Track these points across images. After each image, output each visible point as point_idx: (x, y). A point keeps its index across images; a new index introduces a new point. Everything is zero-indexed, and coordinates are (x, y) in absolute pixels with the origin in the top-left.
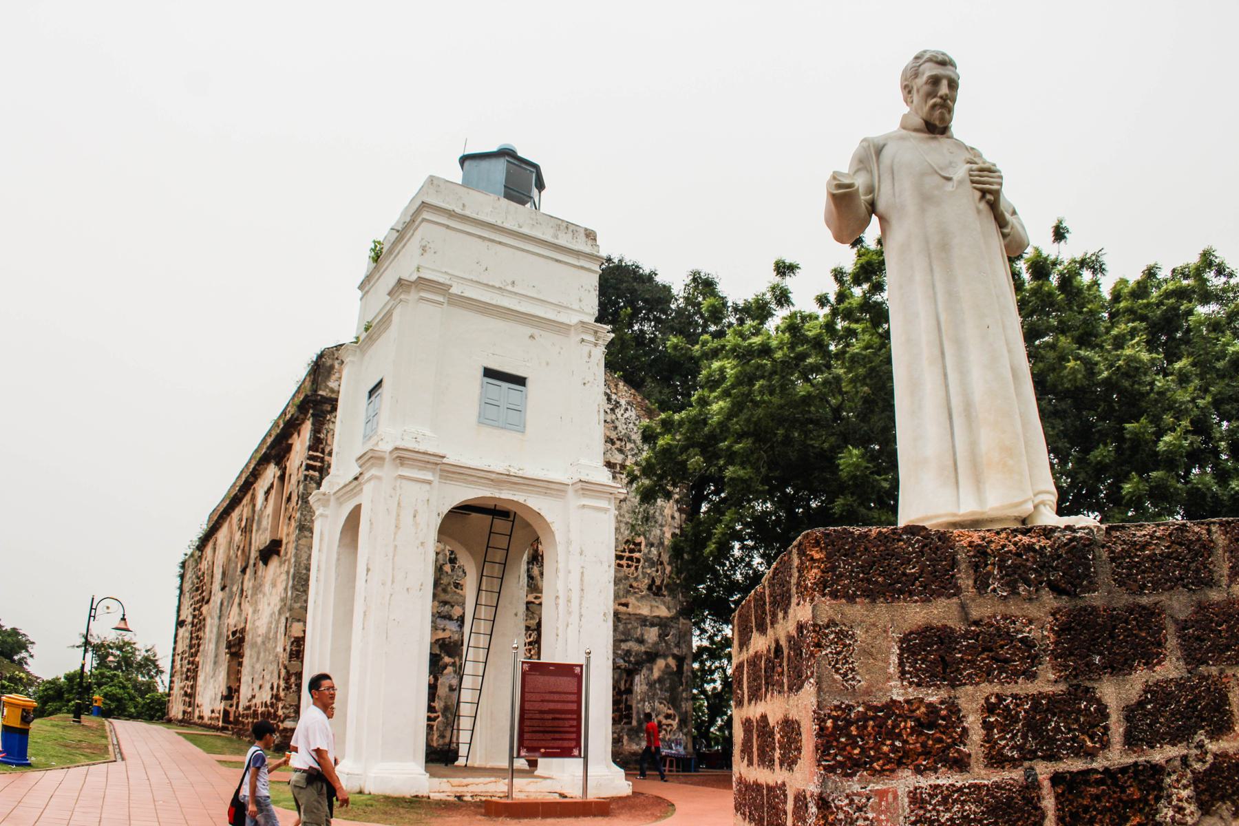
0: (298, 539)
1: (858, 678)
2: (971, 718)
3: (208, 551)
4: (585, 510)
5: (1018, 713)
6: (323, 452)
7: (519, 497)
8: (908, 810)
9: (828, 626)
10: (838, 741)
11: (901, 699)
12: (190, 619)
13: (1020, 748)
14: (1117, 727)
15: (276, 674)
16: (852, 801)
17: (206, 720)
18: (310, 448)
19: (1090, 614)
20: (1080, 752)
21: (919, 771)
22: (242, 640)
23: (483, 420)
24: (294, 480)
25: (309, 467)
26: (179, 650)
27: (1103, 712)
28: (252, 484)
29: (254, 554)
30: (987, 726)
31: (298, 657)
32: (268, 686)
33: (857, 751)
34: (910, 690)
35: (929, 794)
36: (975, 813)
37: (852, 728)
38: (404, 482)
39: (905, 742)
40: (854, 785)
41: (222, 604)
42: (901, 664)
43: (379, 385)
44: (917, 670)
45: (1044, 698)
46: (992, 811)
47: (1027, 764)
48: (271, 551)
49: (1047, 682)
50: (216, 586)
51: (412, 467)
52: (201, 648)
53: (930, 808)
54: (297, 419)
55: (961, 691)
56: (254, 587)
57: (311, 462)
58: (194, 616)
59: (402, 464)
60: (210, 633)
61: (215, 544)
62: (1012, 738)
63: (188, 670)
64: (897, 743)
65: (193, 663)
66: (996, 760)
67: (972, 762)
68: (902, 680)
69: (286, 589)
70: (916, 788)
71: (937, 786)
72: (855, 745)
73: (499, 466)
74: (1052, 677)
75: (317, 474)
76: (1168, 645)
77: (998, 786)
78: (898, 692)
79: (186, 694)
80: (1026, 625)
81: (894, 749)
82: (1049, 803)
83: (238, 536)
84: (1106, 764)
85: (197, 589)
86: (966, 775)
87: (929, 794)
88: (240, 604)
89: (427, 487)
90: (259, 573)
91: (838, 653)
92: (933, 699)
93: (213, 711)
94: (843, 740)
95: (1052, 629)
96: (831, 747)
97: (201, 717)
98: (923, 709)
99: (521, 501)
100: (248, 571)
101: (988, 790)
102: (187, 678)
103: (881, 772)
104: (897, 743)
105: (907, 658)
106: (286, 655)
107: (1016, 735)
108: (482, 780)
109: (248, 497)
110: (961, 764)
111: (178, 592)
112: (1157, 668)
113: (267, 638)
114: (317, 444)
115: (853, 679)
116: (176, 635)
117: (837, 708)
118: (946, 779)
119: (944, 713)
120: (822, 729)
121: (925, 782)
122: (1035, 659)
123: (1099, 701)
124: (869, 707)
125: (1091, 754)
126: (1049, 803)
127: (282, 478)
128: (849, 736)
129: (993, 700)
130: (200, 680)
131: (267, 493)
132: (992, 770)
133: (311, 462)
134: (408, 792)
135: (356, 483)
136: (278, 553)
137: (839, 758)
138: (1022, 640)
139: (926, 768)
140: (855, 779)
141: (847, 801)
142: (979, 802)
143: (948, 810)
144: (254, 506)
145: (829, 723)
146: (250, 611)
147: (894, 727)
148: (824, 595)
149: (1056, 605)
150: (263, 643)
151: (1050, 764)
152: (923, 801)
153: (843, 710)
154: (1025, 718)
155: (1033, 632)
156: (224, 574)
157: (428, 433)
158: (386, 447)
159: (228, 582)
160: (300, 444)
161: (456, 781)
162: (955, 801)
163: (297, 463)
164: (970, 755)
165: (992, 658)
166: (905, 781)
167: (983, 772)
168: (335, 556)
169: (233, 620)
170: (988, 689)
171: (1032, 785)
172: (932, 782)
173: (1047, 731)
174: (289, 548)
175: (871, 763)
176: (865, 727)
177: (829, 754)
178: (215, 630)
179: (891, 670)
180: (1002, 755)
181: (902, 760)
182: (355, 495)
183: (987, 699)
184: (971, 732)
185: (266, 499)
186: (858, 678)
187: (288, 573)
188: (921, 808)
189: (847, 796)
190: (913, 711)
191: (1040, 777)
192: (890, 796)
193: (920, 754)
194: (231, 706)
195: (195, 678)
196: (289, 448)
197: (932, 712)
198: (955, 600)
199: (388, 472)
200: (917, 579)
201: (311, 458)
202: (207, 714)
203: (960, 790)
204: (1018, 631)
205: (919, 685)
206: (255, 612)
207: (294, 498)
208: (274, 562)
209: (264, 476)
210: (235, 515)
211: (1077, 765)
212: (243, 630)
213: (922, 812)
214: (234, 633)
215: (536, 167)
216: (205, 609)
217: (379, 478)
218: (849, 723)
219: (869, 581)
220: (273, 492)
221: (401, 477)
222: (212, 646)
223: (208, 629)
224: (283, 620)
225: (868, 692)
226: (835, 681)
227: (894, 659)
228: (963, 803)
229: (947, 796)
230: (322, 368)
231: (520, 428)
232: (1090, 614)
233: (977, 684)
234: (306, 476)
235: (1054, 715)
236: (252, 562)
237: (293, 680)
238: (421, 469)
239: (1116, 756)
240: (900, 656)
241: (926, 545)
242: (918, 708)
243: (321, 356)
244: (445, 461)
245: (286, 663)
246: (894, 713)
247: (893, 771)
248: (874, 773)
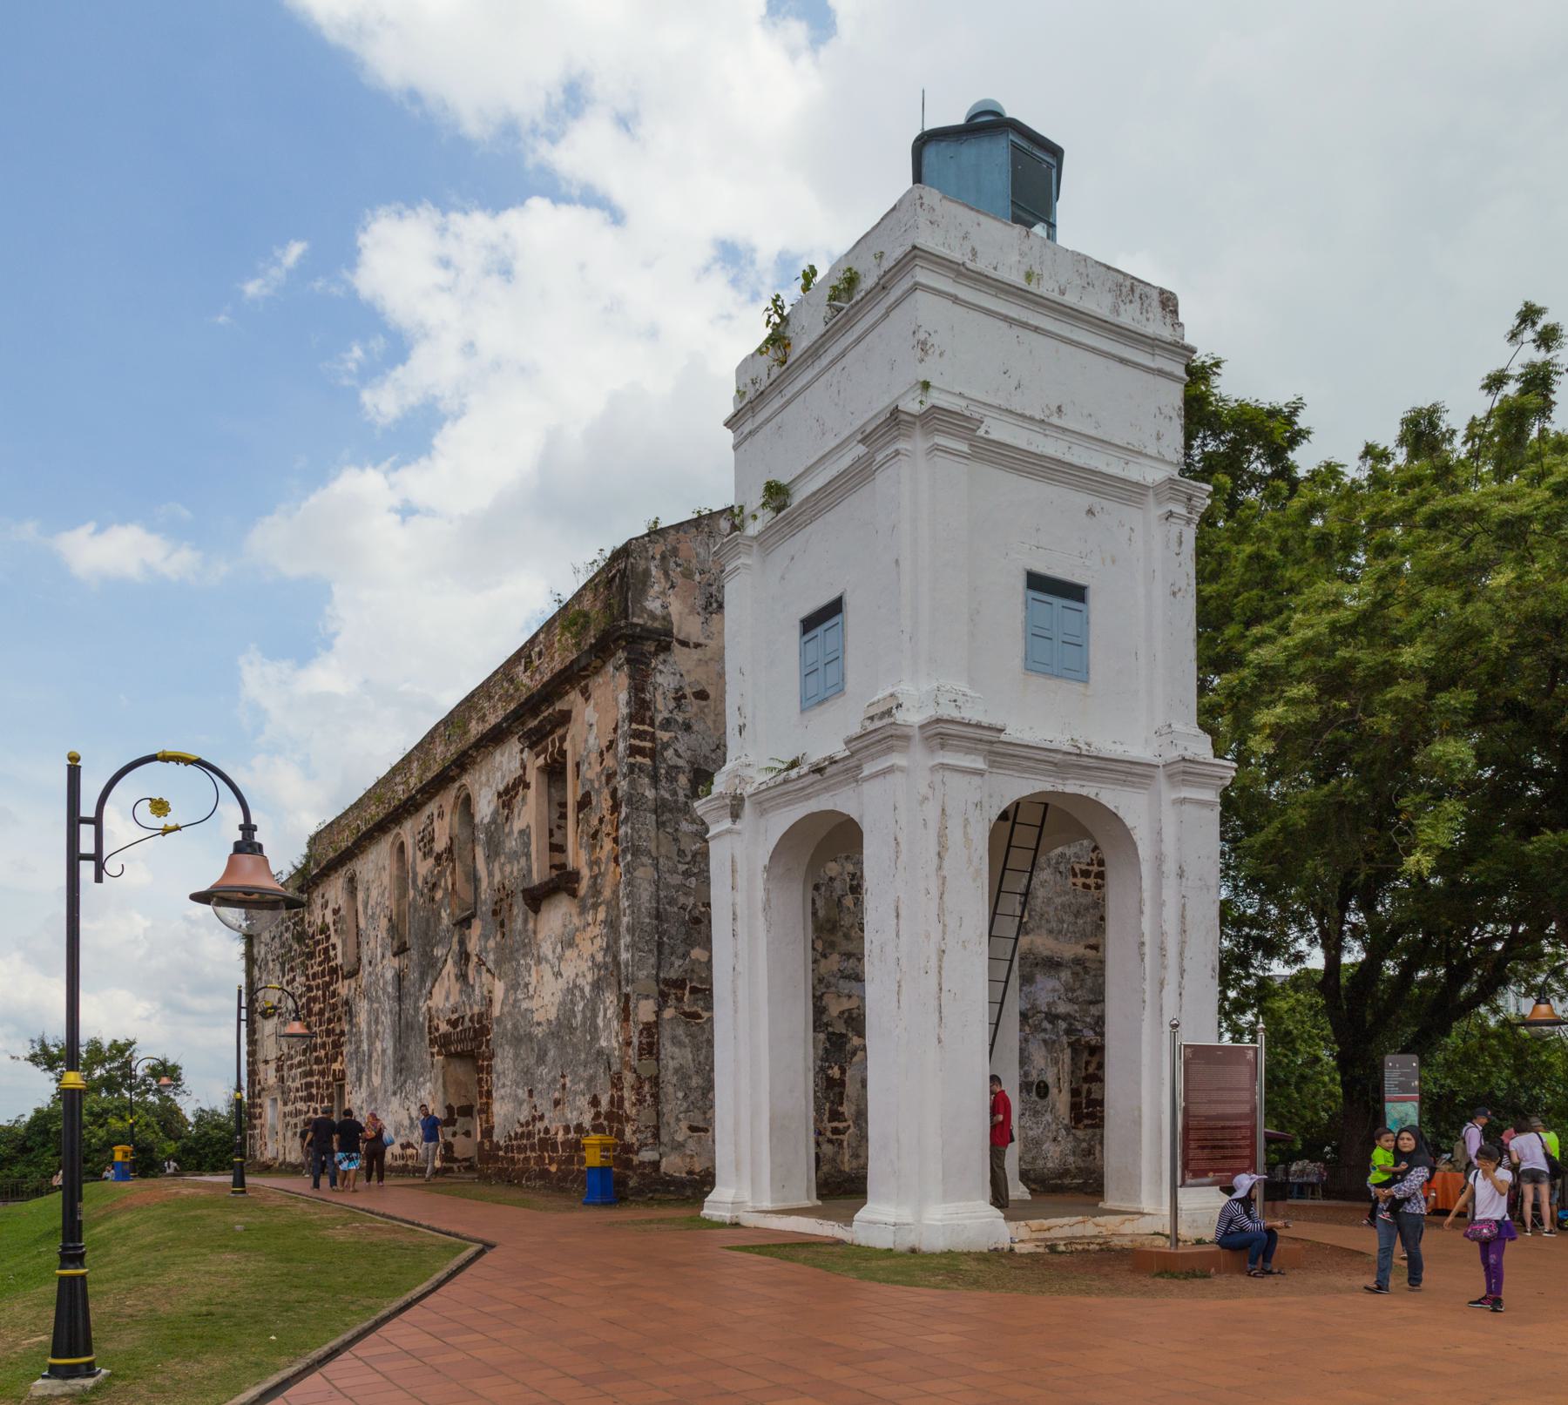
0: (629, 869)
3: (334, 891)
4: (1187, 808)
6: (652, 724)
7: (1089, 790)
15: (603, 1081)
18: (632, 718)
22: (485, 1030)
23: (1033, 665)
24: (592, 771)
26: (269, 1049)
28: (453, 780)
31: (650, 1053)
32: (583, 1102)
38: (947, 773)
41: (400, 978)
51: (958, 749)
52: (345, 1050)
54: (585, 669)
56: (500, 948)
57: (637, 742)
59: (943, 746)
60: (372, 1021)
61: (352, 880)
63: (309, 1086)
65: (322, 1073)
69: (611, 949)
73: (1062, 741)
75: (647, 761)
83: (424, 867)
85: (311, 955)
88: (462, 977)
89: (976, 780)
90: (519, 925)
99: (1092, 796)
100: (477, 924)
102: (310, 1098)
106: (632, 1052)
108: (1065, 1220)
109: (448, 798)
111: (243, 962)
113: (562, 1028)
114: (640, 708)
131: (509, 796)
133: (637, 742)
134: (983, 1245)
135: (818, 776)
136: (573, 894)
146: (499, 988)
150: (553, 1034)
156: (394, 929)
157: (969, 692)
158: (912, 717)
159: (410, 940)
161: (1035, 1223)
163: (595, 741)
168: (760, 895)
169: (443, 997)
178: (387, 1020)
182: (808, 797)
185: (507, 805)
187: (612, 925)
194: (454, 1134)
196: (565, 718)
199: (915, 760)
206: (513, 987)
210: (408, 831)
214: (453, 1024)
217: (902, 769)
221: (944, 766)
222: (385, 1044)
223: (362, 1019)
224: (610, 998)
231: (1079, 673)
234: (632, 767)
236: (485, 909)
237: (646, 1088)
238: (969, 751)
244: (1003, 737)
245: (635, 1063)
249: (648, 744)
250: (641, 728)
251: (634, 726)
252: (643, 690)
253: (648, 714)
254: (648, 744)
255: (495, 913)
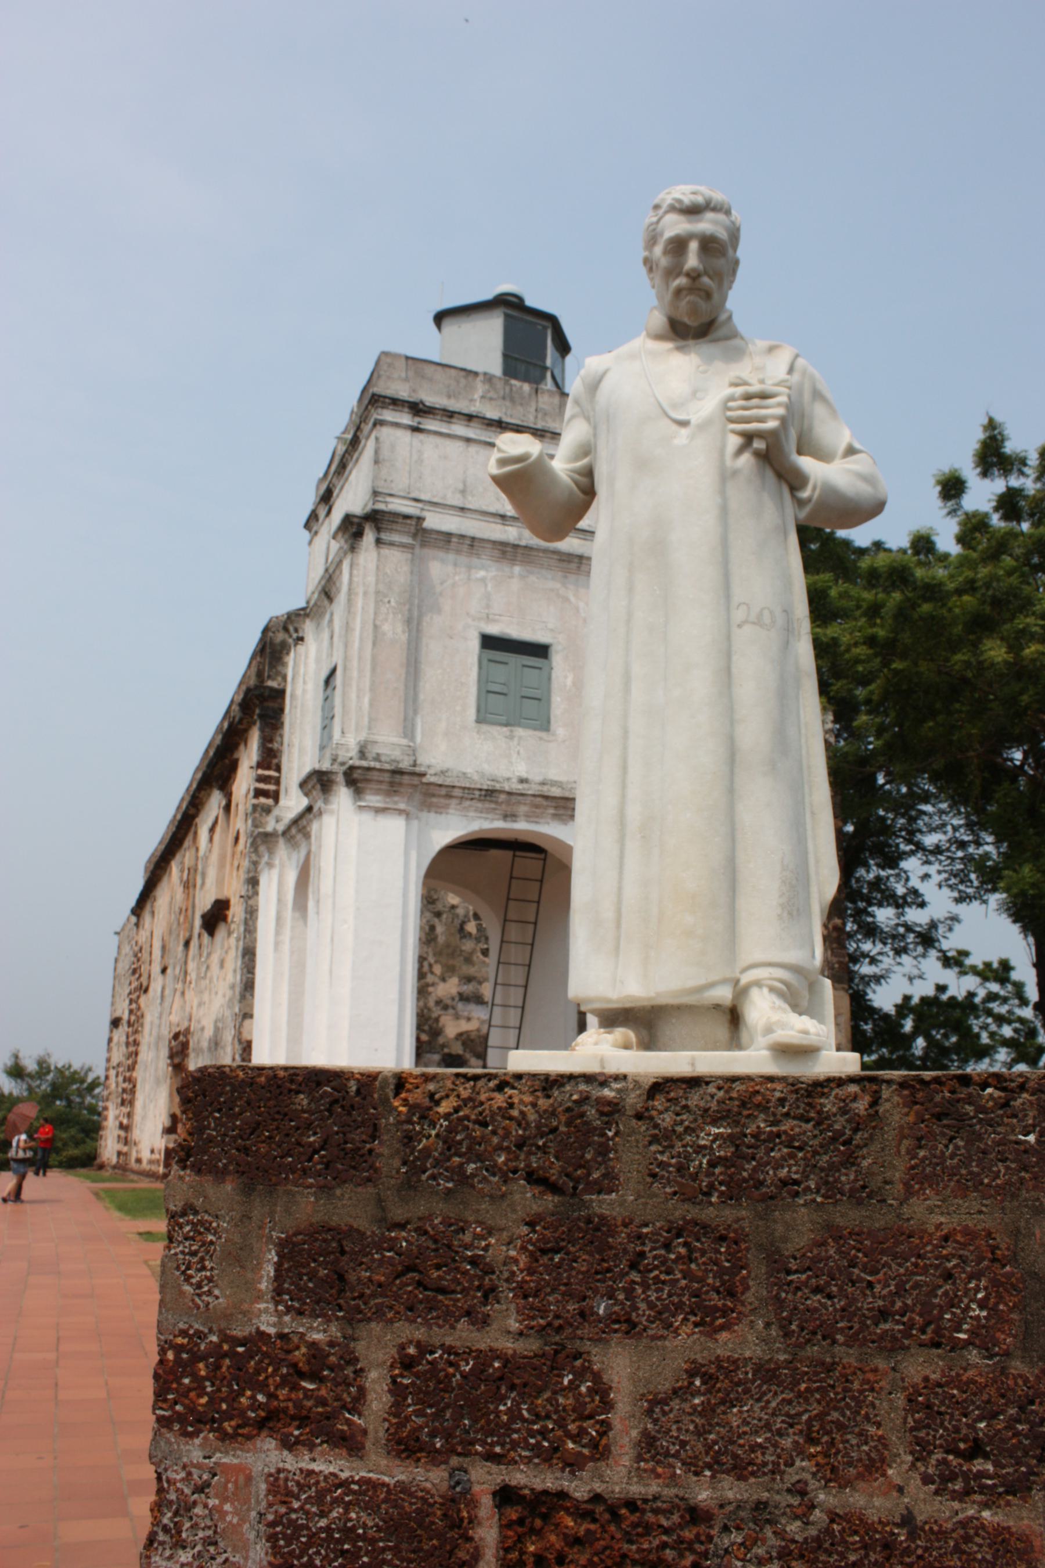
1: (217, 1292)
2: (373, 1375)
5: (449, 1377)
8: (264, 1504)
9: (184, 1214)
10: (180, 1384)
11: (272, 1331)
12: (126, 1017)
13: (448, 1436)
14: (625, 1427)
16: (189, 1474)
17: (145, 1165)
18: (259, 765)
19: (597, 1229)
20: (550, 1456)
21: (288, 1445)
22: (185, 1046)
25: (259, 793)
27: (602, 1390)
28: (194, 817)
29: (198, 922)
30: (397, 1390)
33: (204, 1400)
34: (287, 1319)
35: (298, 1483)
36: (365, 1526)
37: (201, 1365)
39: (271, 1396)
40: (194, 1451)
42: (278, 1277)
43: (333, 671)
44: (300, 1290)
45: (498, 1357)
46: (392, 1527)
47: (455, 1461)
48: (215, 918)
49: (506, 1331)
50: (156, 968)
52: (139, 1058)
53: (296, 1505)
55: (362, 1330)
57: (262, 786)
58: (131, 1012)
62: (437, 1416)
63: (124, 1091)
64: (260, 1398)
66: (406, 1446)
67: (368, 1445)
68: (277, 1303)
70: (279, 1471)
71: (311, 1473)
72: (202, 1393)
74: (514, 1325)
75: (270, 802)
76: (749, 1297)
77: (403, 1488)
78: (267, 1320)
79: (121, 1126)
80: (482, 1237)
81: (255, 1406)
82: (488, 1534)
84: (598, 1487)
86: (358, 1463)
87: (298, 1483)
91: (193, 1254)
92: (317, 1336)
93: (152, 1151)
94: (186, 1381)
95: (523, 1248)
96: (169, 1390)
97: (139, 1161)
98: (304, 1350)
101: (389, 1492)
102: (123, 1103)
103: (233, 1437)
104: (260, 1398)
105: (288, 1270)
107: (443, 1410)
110: (351, 1444)
112: (724, 1335)
115: (209, 1293)
116: (110, 1040)
117: (184, 1333)
118: (328, 1464)
119: (333, 1359)
120: (161, 1362)
121: (291, 1462)
122: (490, 1293)
123: (597, 1377)
124: (225, 1338)
125: (573, 1465)
126: (488, 1534)
127: (227, 808)
128: (195, 1376)
129: (411, 1351)
130: (139, 1104)
131: (212, 830)
132: (398, 1462)
133: (262, 786)
136: (224, 918)
137: (178, 1408)
138: (474, 1261)
139: (298, 1442)
140: (197, 1441)
141: (183, 1475)
142: (371, 1507)
143: (323, 1514)
144: (197, 849)
145: (170, 1355)
147: (258, 1372)
148: (184, 1168)
149: (536, 1208)
151: (494, 1468)
152: (289, 1493)
153: (191, 1337)
154: (460, 1386)
155: (497, 1250)
156: (164, 948)
160: (249, 755)
162: (337, 1501)
164: (365, 1432)
165: (419, 1284)
166: (266, 1456)
167: (384, 1462)
170: (410, 1332)
171: (459, 1498)
172: (303, 1465)
173: (498, 1413)
174: (236, 912)
175: (221, 1421)
176: (217, 1367)
177: (165, 1400)
179: (263, 1286)
180: (417, 1439)
181: (268, 1421)
183: (402, 1347)
184: (371, 1396)
185: (211, 840)
186: (217, 1292)
188: (284, 1503)
189: (184, 1467)
190: (289, 1352)
191: (476, 1488)
192: (241, 1479)
193: (293, 1418)
195: (131, 1103)
197: (314, 1356)
198: (371, 1189)
200: (316, 1152)
201: (260, 779)
202: (146, 1155)
203: (345, 1484)
204: (467, 1247)
205: (300, 1313)
207: (242, 841)
208: (221, 932)
209: (207, 807)
211: (548, 1480)
212: (187, 1032)
213: (283, 1510)
215: (553, 321)
216: (142, 1000)
218: (197, 1357)
219: (246, 1150)
220: (218, 829)
225: (228, 1317)
226: (182, 1293)
227: (270, 1270)
228: (347, 1507)
229: (326, 1491)
230: (273, 649)
232: (597, 1229)
233: (391, 1321)
234: (255, 807)
235: (512, 1387)
239: (619, 1477)
240: (278, 1267)
241: (336, 1101)
242: (298, 1348)
243: (266, 630)
246: (259, 1350)
247: (249, 1437)
248: (224, 1437)
249: (272, 787)
250: (267, 773)
251: (260, 772)
252: (271, 741)
253: (275, 761)
254: (272, 787)
255: (200, 935)
